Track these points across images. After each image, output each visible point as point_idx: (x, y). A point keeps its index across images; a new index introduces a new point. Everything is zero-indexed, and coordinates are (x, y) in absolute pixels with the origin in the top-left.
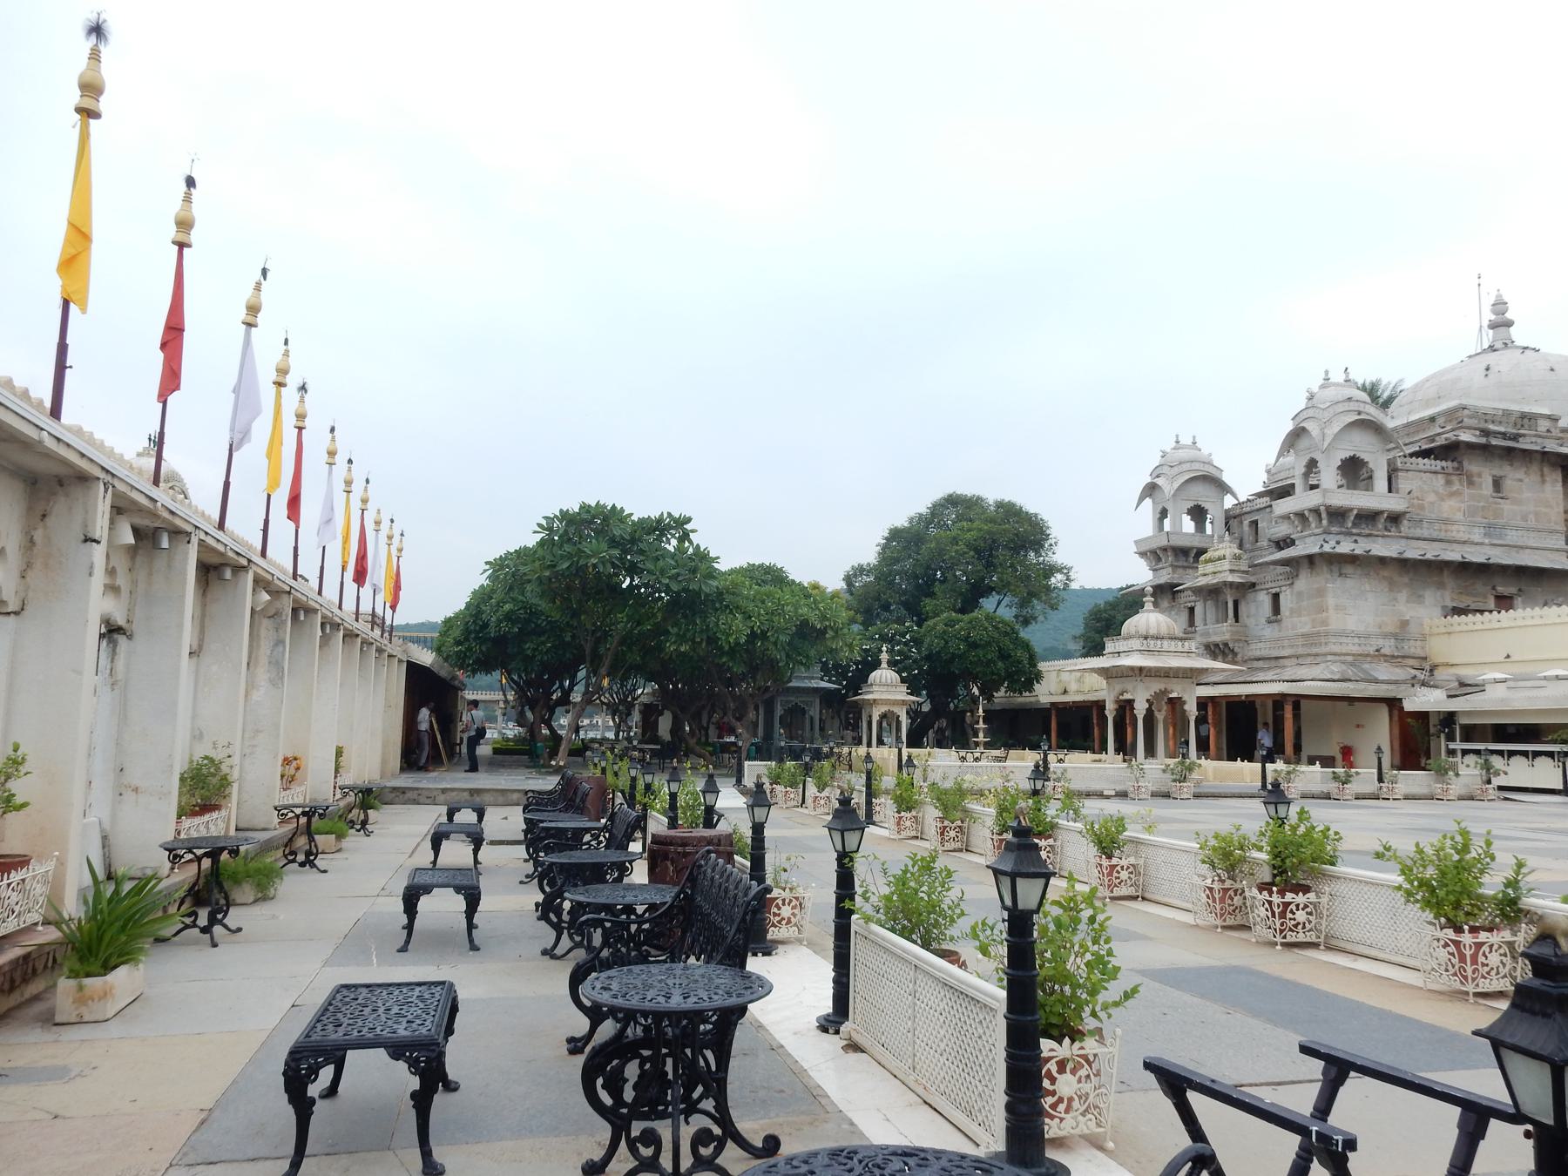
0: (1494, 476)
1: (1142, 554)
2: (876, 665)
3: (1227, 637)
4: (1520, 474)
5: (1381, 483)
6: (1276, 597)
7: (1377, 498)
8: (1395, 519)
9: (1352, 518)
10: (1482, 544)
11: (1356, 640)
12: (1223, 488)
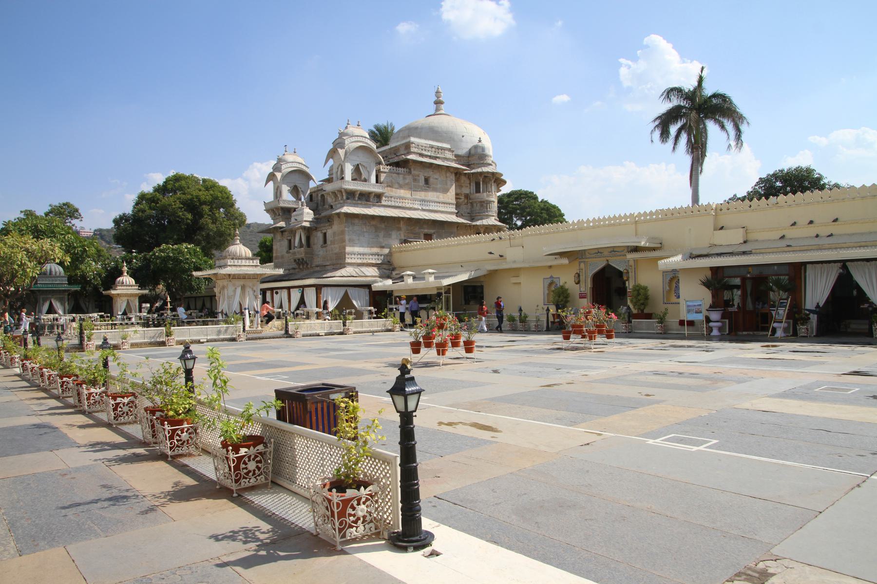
0: (425, 176)
1: (267, 211)
2: (121, 274)
3: (303, 256)
6: (325, 235)
7: (371, 186)
8: (379, 196)
9: (358, 195)
11: (359, 256)
12: (308, 177)
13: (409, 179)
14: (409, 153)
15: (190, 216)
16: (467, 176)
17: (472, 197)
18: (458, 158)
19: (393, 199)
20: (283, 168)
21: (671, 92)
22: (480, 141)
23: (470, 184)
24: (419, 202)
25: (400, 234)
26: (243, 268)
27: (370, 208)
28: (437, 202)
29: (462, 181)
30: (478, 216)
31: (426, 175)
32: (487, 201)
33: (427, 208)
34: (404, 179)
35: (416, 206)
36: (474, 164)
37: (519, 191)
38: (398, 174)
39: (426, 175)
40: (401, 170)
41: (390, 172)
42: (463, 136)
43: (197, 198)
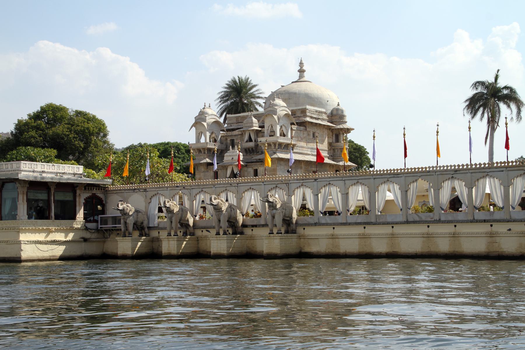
16: (331, 130)
20: (207, 118)
21: (476, 84)
22: (338, 105)
23: (332, 135)
24: (310, 150)
30: (338, 158)
31: (313, 131)
35: (309, 153)
36: (336, 122)
38: (301, 131)
39: (313, 131)
40: (302, 128)
43: (87, 130)
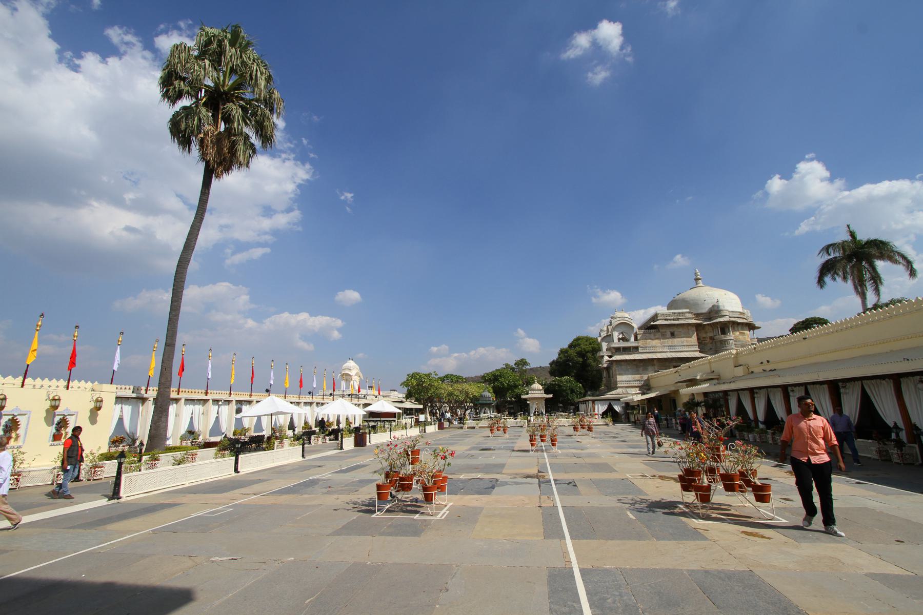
4: (680, 330)
5: (632, 339)
7: (632, 343)
10: (667, 352)
13: (659, 335)
14: (657, 320)
15: (581, 360)
17: (715, 338)
18: (698, 315)
19: (647, 348)
21: (827, 249)
25: (654, 368)
26: (536, 395)
27: (631, 354)
28: (682, 346)
29: (707, 329)
31: (672, 330)
32: (725, 340)
33: (674, 350)
34: (655, 335)
37: (812, 318)
41: (644, 333)
42: (705, 301)
